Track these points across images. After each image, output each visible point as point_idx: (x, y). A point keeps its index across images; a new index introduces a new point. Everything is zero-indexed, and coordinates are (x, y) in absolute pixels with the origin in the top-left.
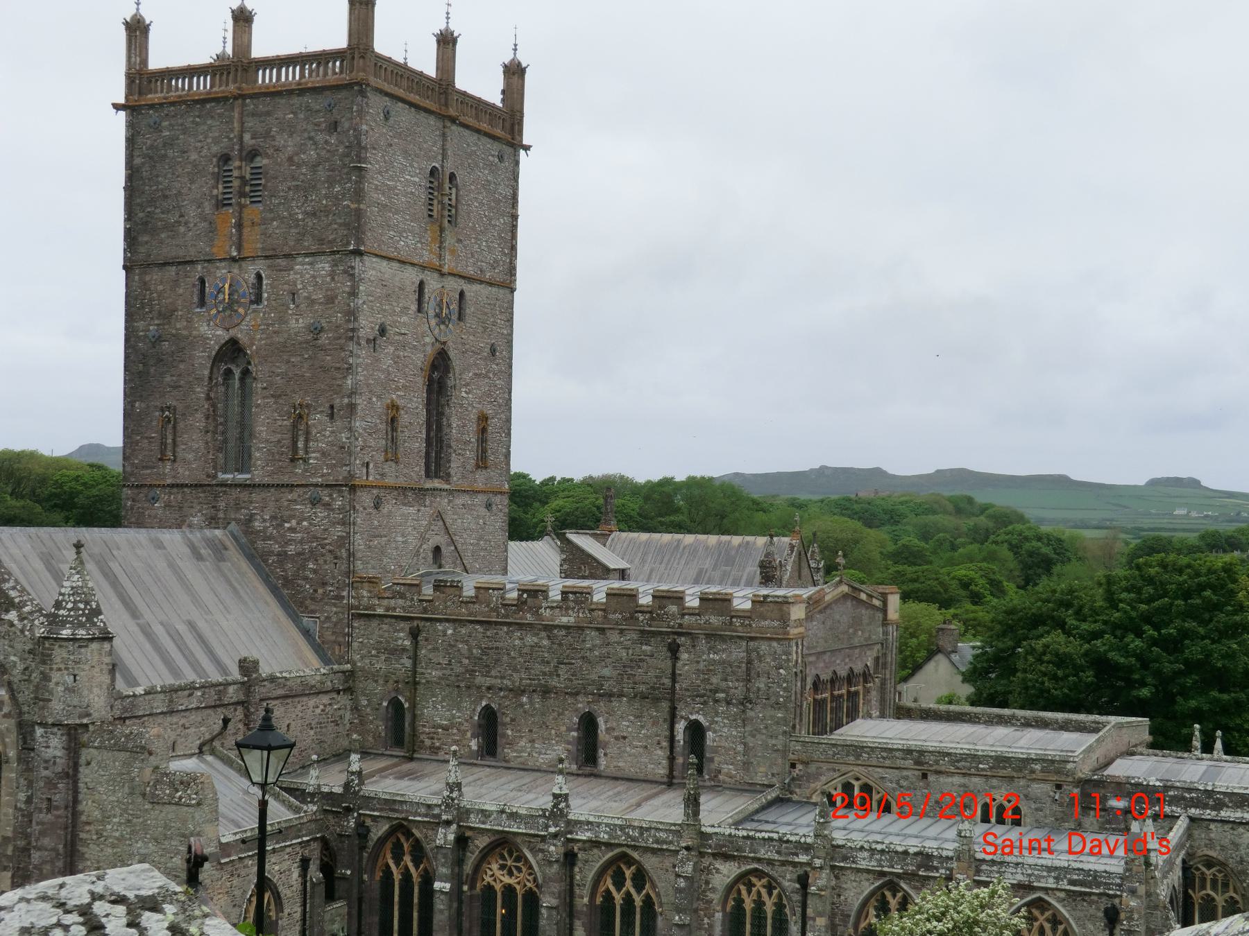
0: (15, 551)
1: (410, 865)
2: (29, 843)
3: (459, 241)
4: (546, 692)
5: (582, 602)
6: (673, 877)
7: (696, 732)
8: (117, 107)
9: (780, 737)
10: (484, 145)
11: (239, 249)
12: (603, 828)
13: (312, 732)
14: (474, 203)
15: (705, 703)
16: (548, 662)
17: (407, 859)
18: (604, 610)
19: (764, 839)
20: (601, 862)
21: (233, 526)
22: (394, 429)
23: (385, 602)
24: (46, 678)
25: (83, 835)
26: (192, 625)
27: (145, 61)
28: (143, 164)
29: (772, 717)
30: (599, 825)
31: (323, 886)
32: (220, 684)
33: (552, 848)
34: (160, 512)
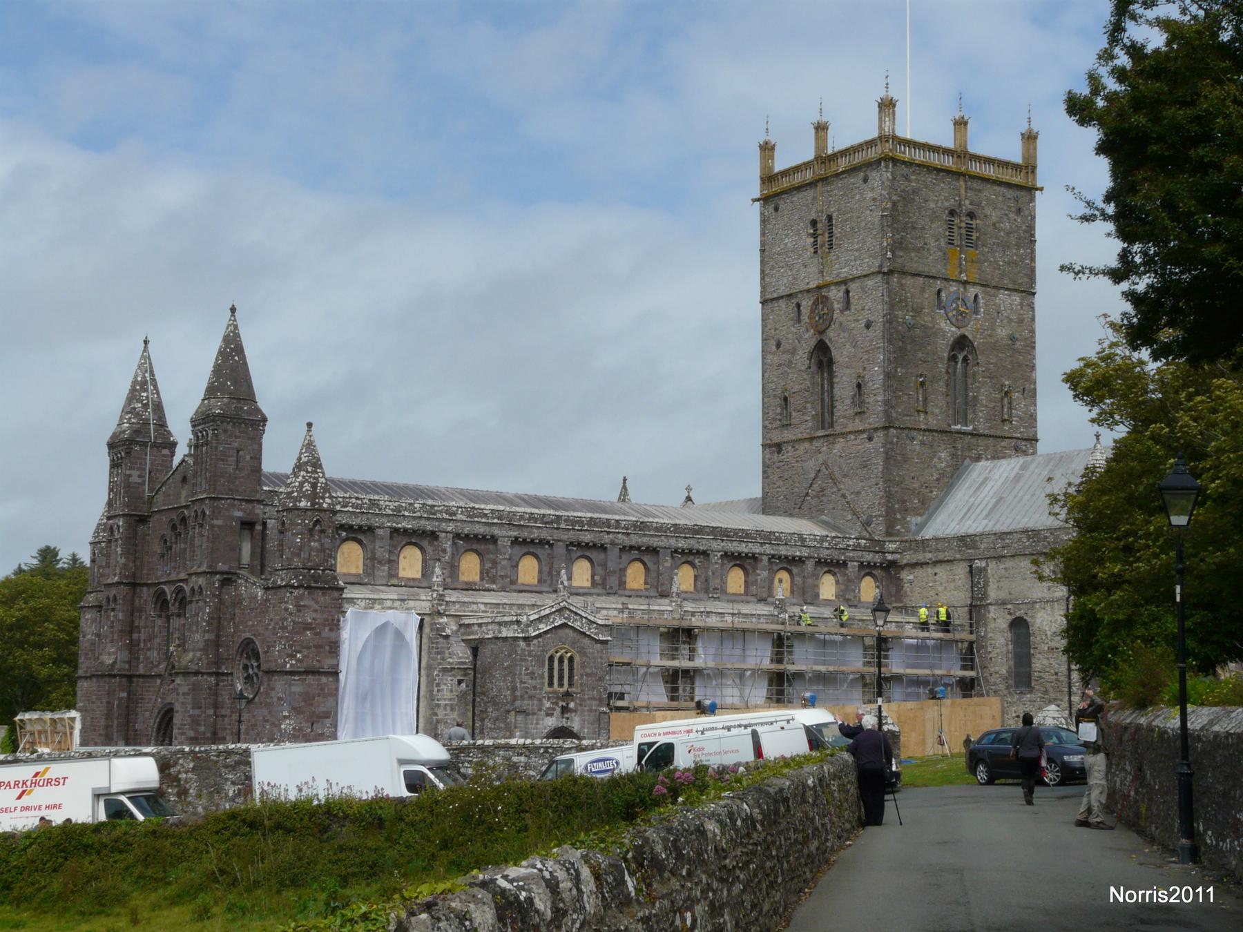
28: (899, 201)
34: (918, 448)
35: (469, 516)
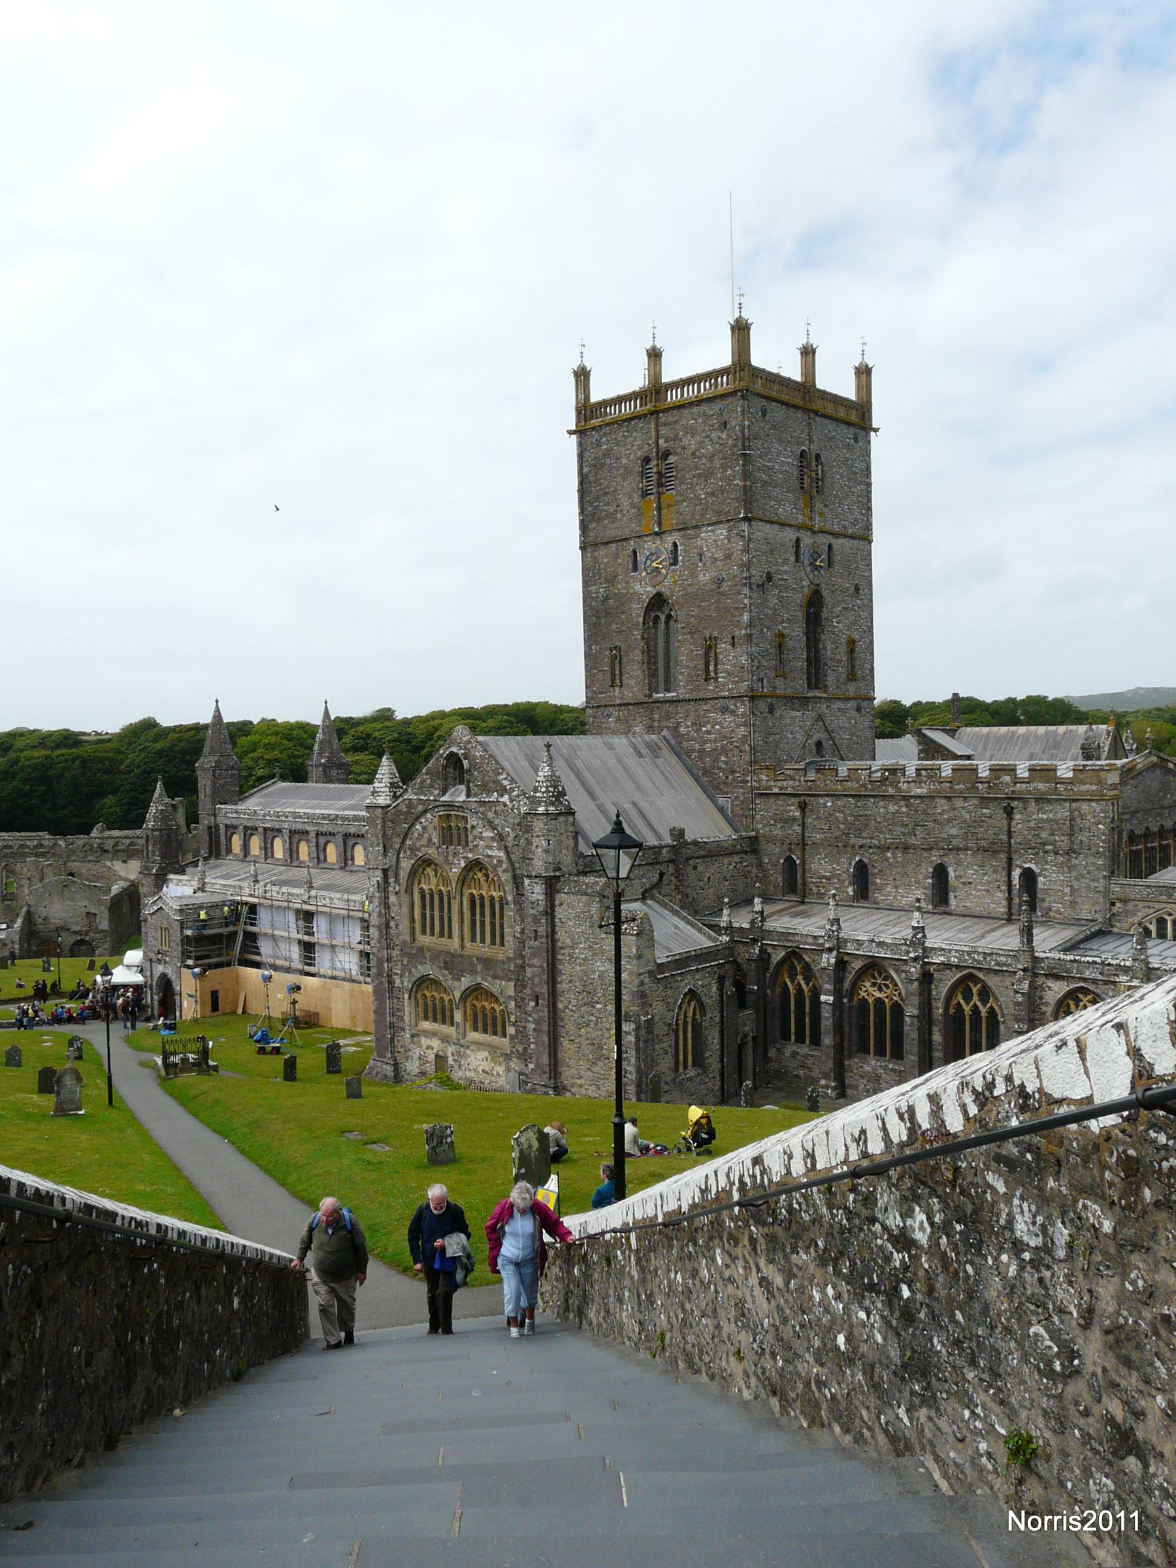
0: (507, 753)
1: (802, 982)
2: (524, 962)
3: (826, 506)
4: (906, 848)
5: (932, 777)
6: (1012, 993)
7: (1029, 878)
8: (570, 433)
9: (1101, 880)
10: (842, 431)
11: (660, 525)
12: (953, 953)
13: (727, 883)
14: (837, 478)
15: (1037, 854)
16: (907, 825)
17: (800, 978)
18: (950, 782)
19: (1088, 962)
20: (953, 980)
21: (665, 732)
22: (781, 652)
23: (779, 784)
24: (529, 843)
25: (559, 957)
26: (635, 805)
27: (587, 397)
29: (1093, 864)
30: (950, 951)
31: (735, 998)
32: (656, 847)
33: (913, 970)
35: (294, 818)
